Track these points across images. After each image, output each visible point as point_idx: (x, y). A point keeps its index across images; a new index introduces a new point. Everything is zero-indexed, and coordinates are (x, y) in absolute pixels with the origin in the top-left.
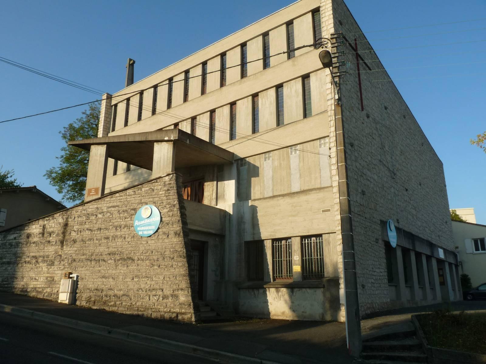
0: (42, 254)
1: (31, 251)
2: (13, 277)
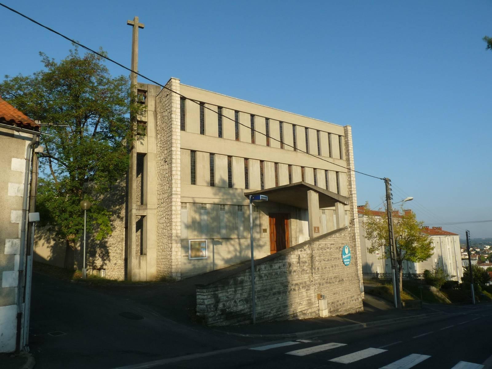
0: (300, 281)
1: (296, 278)
2: (286, 306)
